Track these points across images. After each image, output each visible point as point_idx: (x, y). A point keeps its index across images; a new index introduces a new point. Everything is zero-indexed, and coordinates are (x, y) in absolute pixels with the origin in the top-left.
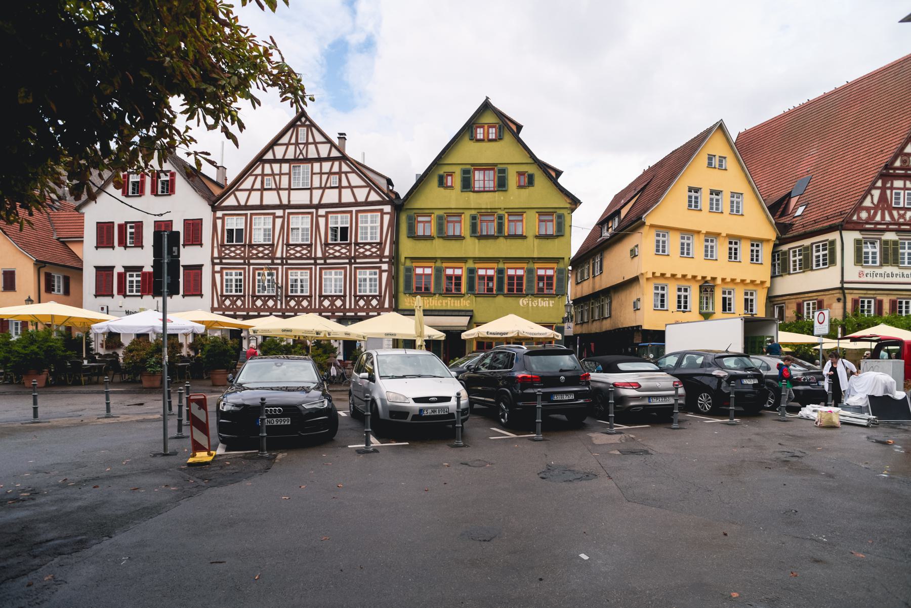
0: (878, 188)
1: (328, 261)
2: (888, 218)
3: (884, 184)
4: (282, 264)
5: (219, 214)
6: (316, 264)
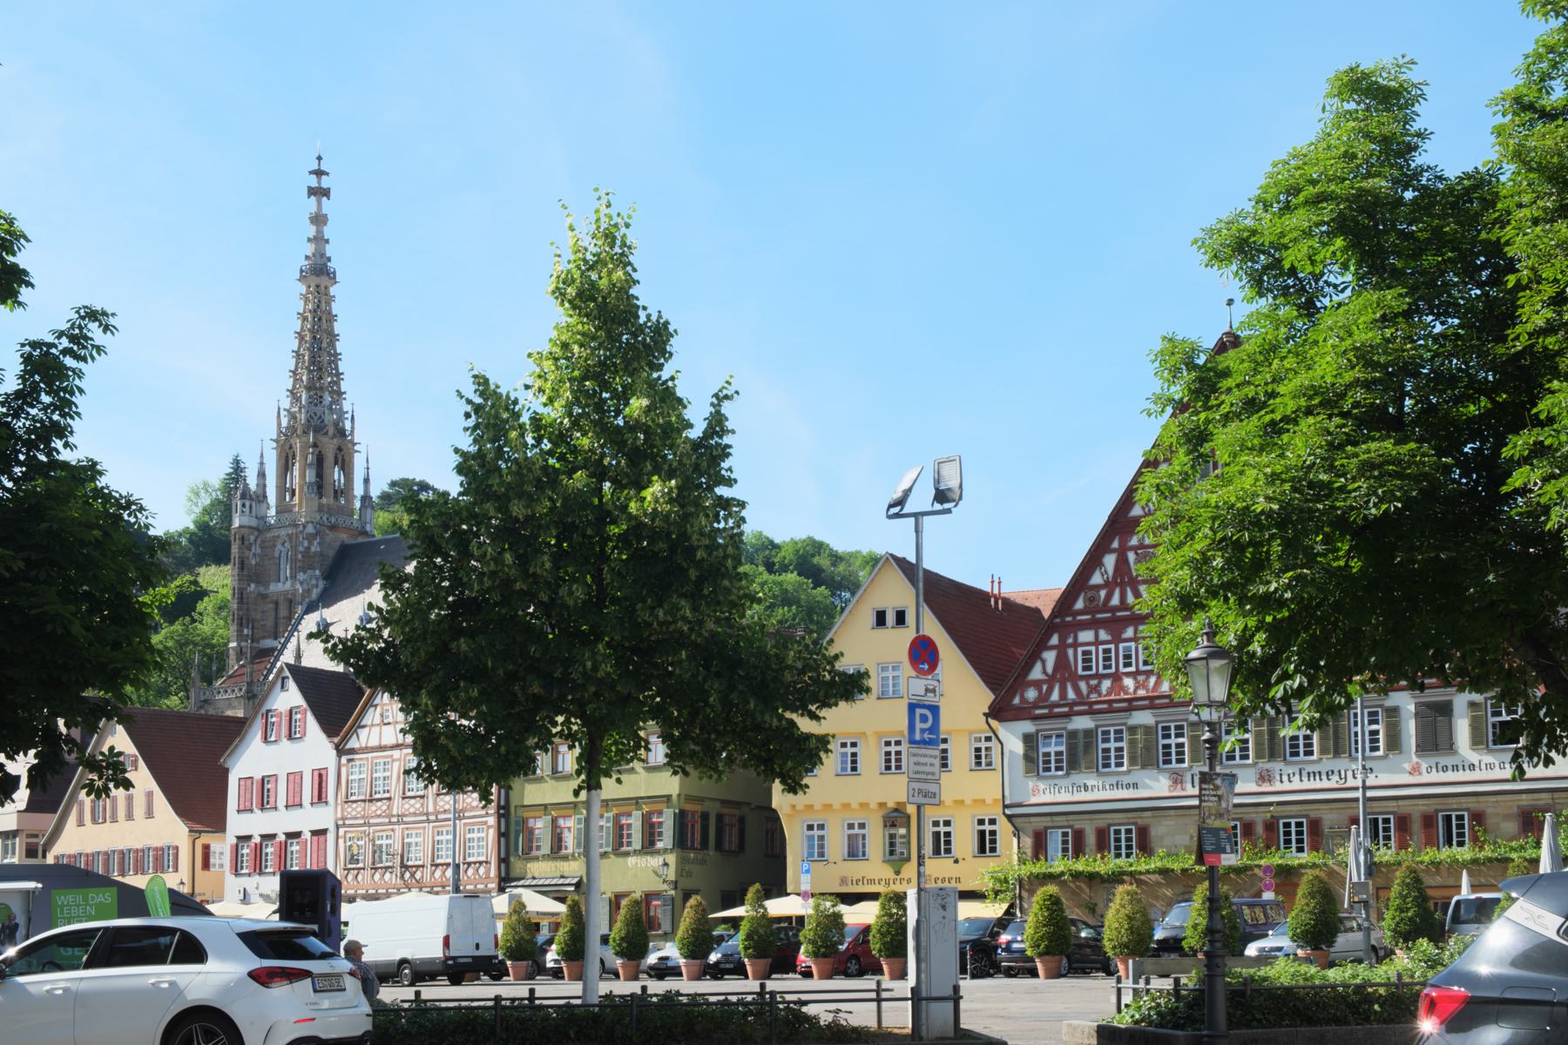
0: (1052, 648)
1: (440, 817)
2: (1071, 695)
3: (1062, 640)
4: (398, 823)
5: (344, 760)
6: (428, 821)
